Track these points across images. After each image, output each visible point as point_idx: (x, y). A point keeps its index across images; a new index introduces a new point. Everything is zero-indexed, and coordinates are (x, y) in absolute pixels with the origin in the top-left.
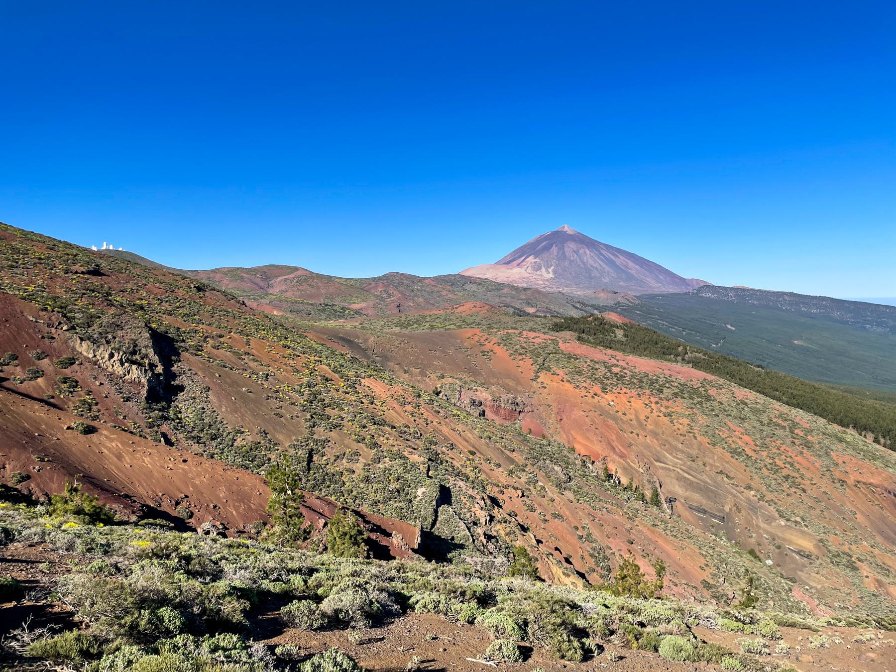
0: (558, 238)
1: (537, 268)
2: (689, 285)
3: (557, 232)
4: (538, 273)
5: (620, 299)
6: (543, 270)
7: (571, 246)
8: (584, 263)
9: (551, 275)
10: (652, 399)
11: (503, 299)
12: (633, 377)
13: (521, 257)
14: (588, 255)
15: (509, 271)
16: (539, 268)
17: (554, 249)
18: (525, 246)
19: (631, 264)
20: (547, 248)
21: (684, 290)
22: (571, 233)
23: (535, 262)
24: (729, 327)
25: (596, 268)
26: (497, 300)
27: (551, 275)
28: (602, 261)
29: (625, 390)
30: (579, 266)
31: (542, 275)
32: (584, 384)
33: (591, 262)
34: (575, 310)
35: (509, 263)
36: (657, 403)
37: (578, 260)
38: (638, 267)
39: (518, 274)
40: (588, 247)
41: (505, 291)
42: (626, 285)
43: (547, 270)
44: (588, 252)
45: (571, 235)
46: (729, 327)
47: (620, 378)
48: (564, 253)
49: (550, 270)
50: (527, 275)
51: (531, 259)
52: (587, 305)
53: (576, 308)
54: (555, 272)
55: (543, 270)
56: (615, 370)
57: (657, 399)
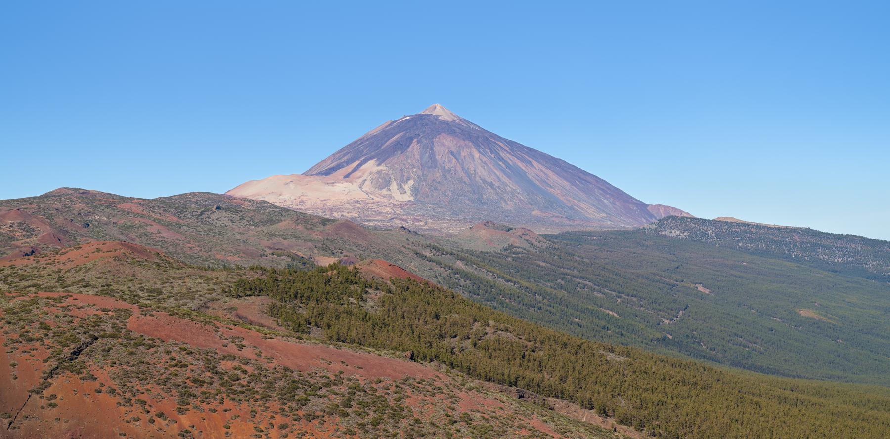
0: (420, 128)
1: (383, 183)
2: (651, 216)
3: (421, 117)
4: (384, 191)
5: (513, 240)
6: (394, 186)
7: (444, 144)
8: (469, 175)
9: (408, 197)
10: (279, 420)
11: (275, 240)
12: (255, 378)
13: (352, 160)
14: (476, 161)
15: (329, 188)
16: (386, 184)
17: (415, 148)
18: (361, 141)
19: (553, 177)
20: (402, 146)
21: (627, 224)
23: (379, 172)
24: (701, 288)
25: (492, 185)
26: (265, 242)
27: (408, 197)
29: (228, 404)
30: (461, 181)
31: (390, 197)
32: (143, 397)
33: (481, 172)
34: (418, 261)
35: (328, 173)
36: (283, 427)
37: (459, 170)
38: (566, 184)
39: (342, 196)
40: (477, 146)
41: (285, 224)
42: (543, 215)
43: (400, 187)
44: (476, 155)
45: (447, 123)
46: (701, 288)
47: (229, 382)
48: (432, 156)
49: (407, 187)
50: (360, 196)
51: (371, 166)
52: (443, 252)
53: (423, 257)
54: (415, 191)
55: (394, 186)
56: (225, 366)
57: (288, 420)
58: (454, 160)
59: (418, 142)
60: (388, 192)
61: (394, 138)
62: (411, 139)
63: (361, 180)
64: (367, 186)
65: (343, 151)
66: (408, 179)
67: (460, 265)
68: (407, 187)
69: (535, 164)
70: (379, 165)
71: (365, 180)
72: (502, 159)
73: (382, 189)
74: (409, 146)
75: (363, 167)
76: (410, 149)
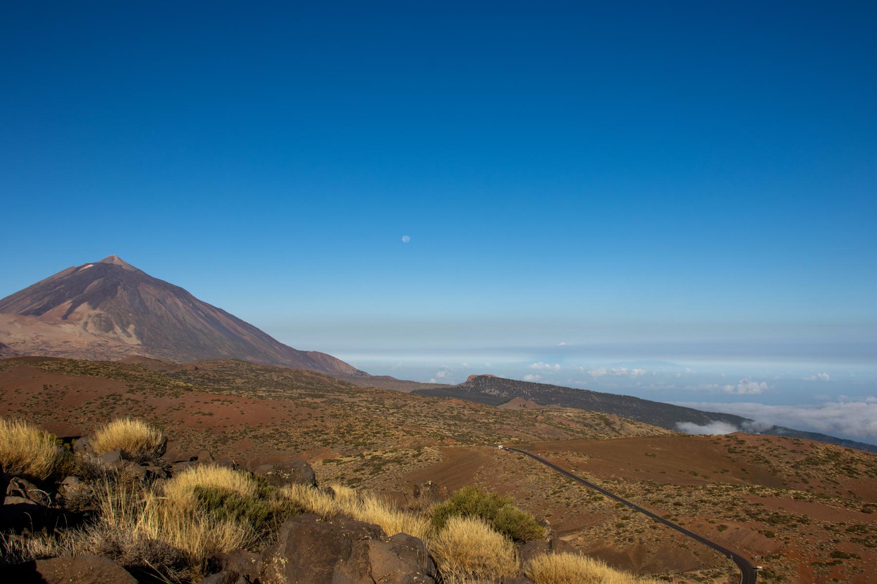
4: (111, 334)
43: (125, 331)
44: (181, 304)
54: (140, 336)
55: (118, 329)
58: (163, 308)
59: (125, 289)
60: (115, 336)
61: (95, 283)
63: (82, 322)
64: (91, 328)
66: (129, 324)
70: (94, 308)
71: (86, 323)
72: (199, 309)
73: (107, 332)
74: (116, 293)
75: (78, 309)
76: (119, 295)
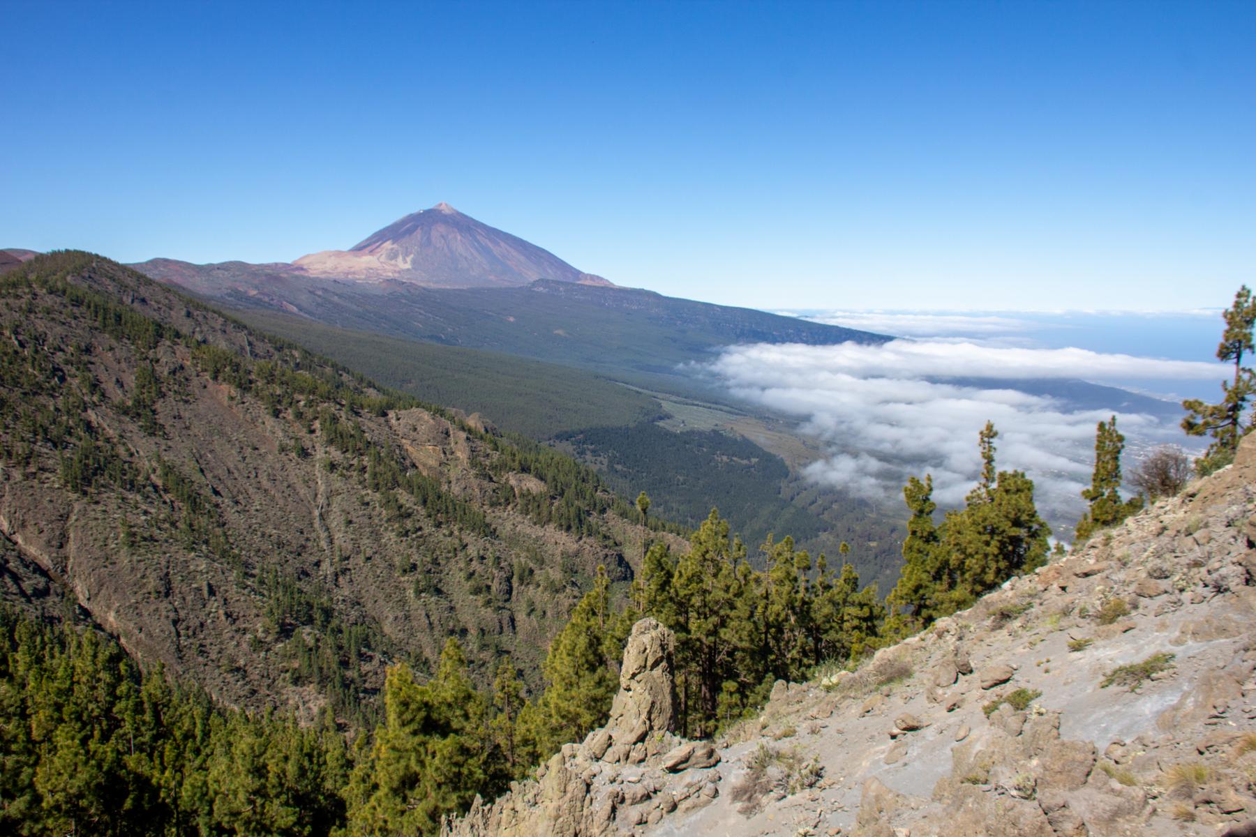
0: (429, 219)
1: (393, 256)
3: (429, 213)
6: (400, 258)
14: (459, 243)
17: (418, 234)
20: (410, 232)
22: (447, 211)
27: (408, 266)
28: (477, 250)
38: (522, 258)
45: (445, 216)
49: (409, 259)
51: (388, 245)
54: (414, 262)
55: (400, 258)
62: (416, 227)
64: (383, 259)
65: (375, 235)
67: (336, 299)
68: (409, 259)
69: (502, 244)
72: (478, 241)
